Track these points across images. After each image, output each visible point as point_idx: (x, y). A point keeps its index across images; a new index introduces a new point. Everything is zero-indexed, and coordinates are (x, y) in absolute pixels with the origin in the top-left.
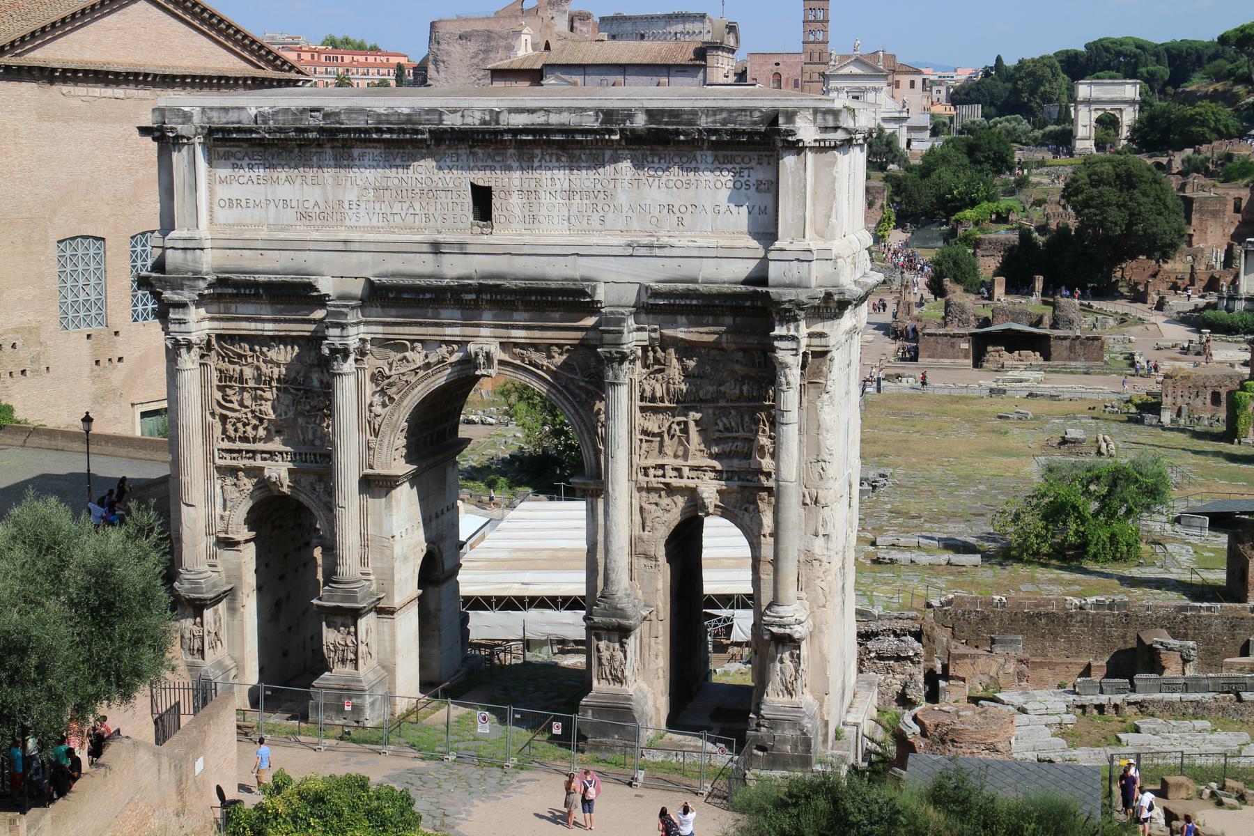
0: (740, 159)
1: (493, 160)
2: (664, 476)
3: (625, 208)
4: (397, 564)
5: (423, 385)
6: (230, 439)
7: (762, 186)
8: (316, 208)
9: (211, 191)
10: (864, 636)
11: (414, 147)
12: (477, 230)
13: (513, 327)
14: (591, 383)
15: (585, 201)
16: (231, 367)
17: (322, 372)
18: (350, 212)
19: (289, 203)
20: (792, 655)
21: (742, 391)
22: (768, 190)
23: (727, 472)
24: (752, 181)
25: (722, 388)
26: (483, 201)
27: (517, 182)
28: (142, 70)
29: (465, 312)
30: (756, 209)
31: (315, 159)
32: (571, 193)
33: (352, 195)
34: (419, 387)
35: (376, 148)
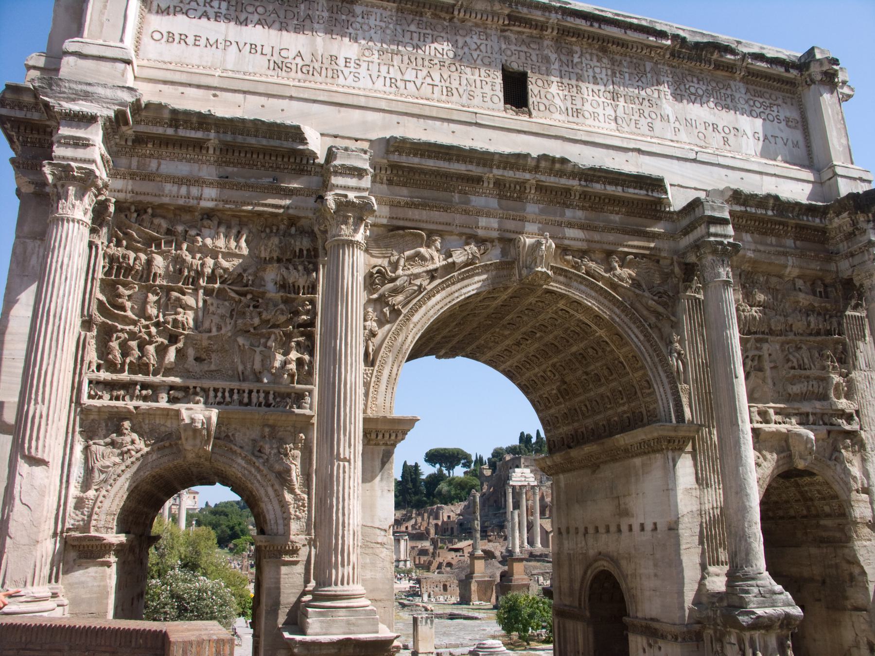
0: (767, 96)
1: (528, 46)
3: (672, 119)
5: (443, 294)
7: (790, 123)
8: (298, 60)
11: (435, 16)
12: (511, 114)
13: (571, 225)
14: (659, 303)
15: (631, 106)
17: (287, 268)
18: (346, 71)
19: (259, 49)
21: (809, 324)
23: (814, 414)
24: (782, 117)
29: (504, 202)
30: (790, 142)
31: (302, 6)
34: (438, 297)
35: (385, 9)
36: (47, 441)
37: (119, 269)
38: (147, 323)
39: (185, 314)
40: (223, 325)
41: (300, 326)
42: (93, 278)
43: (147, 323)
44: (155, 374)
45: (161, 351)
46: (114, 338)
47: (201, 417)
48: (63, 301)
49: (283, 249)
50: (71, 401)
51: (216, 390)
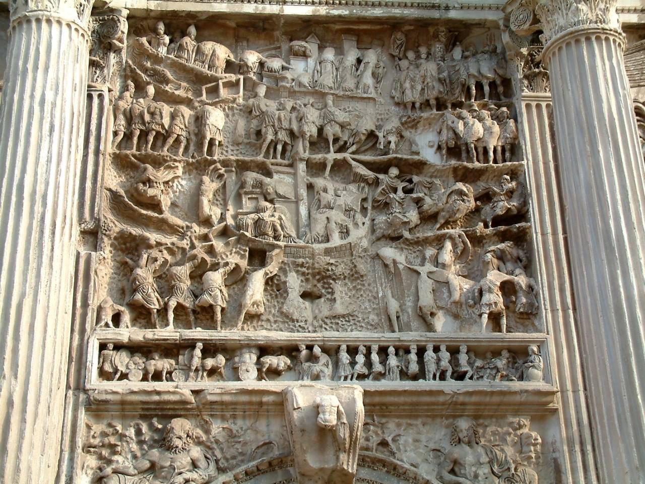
6: (142, 315)
36: (24, 457)
37: (144, 135)
38: (204, 230)
39: (275, 210)
40: (351, 226)
41: (497, 221)
42: (97, 152)
43: (205, 231)
44: (229, 322)
45: (237, 279)
46: (143, 261)
47: (336, 402)
48: (48, 171)
49: (447, 82)
50: (68, 387)
51: (353, 351)
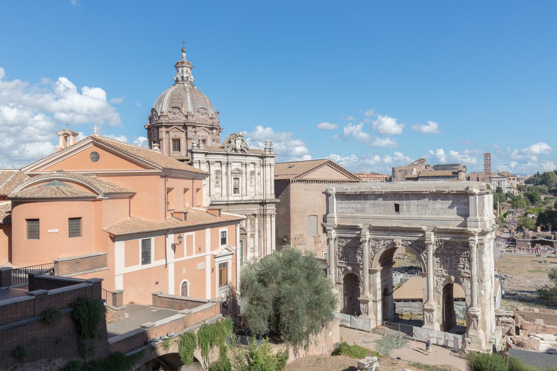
0: (459, 197)
2: (442, 273)
4: (378, 290)
9: (337, 205)
10: (498, 317)
16: (341, 244)
20: (476, 319)
22: (467, 205)
24: (463, 202)
25: (456, 252)
26: (397, 208)
27: (405, 203)
28: (326, 180)
32: (418, 205)
33: (367, 206)
34: (383, 249)
